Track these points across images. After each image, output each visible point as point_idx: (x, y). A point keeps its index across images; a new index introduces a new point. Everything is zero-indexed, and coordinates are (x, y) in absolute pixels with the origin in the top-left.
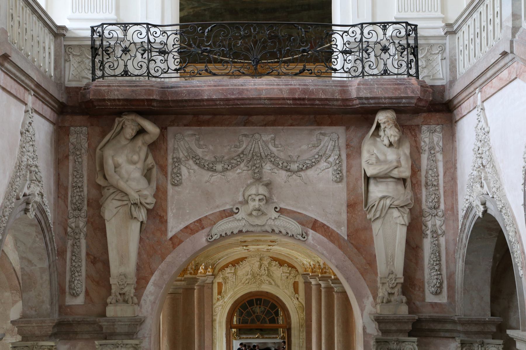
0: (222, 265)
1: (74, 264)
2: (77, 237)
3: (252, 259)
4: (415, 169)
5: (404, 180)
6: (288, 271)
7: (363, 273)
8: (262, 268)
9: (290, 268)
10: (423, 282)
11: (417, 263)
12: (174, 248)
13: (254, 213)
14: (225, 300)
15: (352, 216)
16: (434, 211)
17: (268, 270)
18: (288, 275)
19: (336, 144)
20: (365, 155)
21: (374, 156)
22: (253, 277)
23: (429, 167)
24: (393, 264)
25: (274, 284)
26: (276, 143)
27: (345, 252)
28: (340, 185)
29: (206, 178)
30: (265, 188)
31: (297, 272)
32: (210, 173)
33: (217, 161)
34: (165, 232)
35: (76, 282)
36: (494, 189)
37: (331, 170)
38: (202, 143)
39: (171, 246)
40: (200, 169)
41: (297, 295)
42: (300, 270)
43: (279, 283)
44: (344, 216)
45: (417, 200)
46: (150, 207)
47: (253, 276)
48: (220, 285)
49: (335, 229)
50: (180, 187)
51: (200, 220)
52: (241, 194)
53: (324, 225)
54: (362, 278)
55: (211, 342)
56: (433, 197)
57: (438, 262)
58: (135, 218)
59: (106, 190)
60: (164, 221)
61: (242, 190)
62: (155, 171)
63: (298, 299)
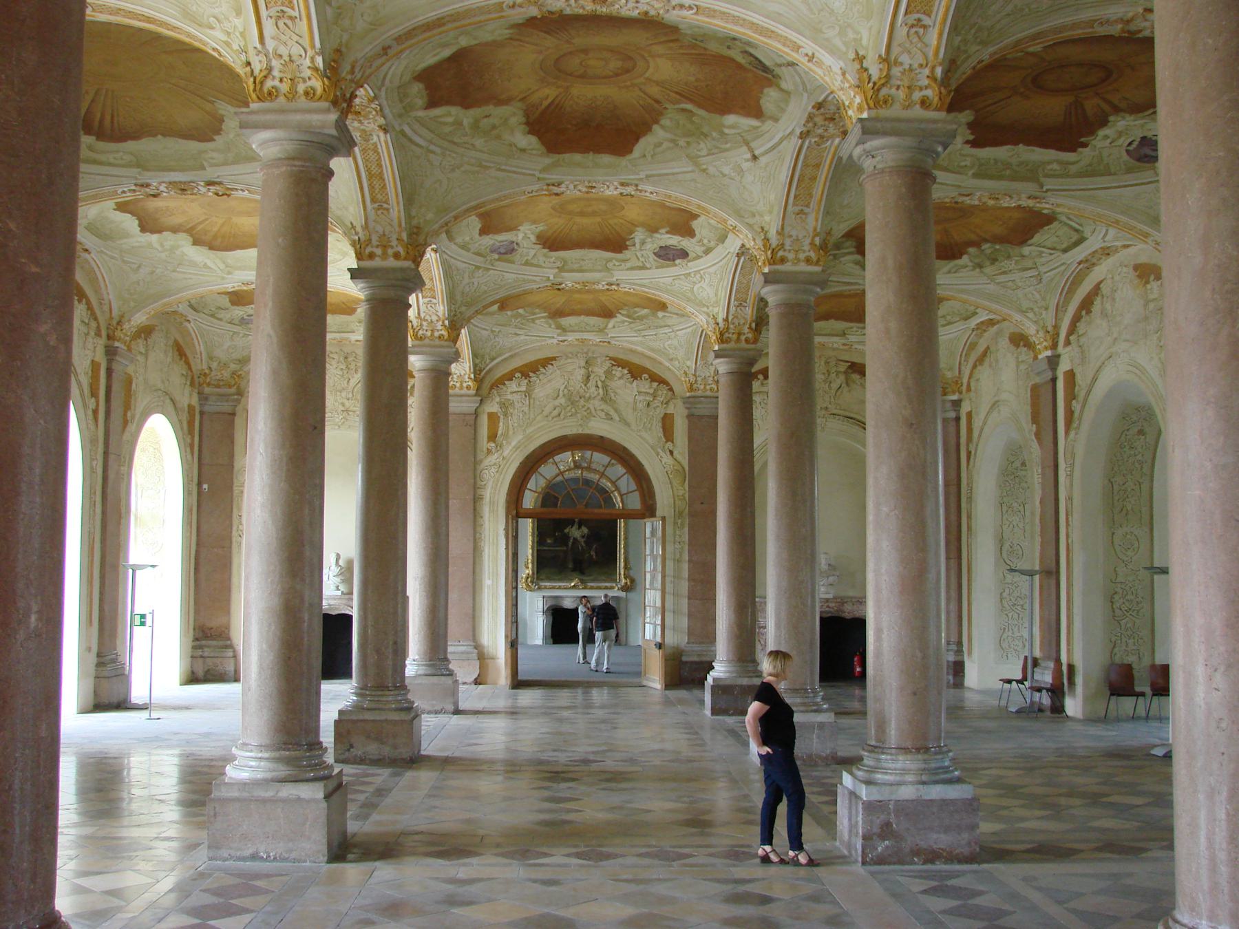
3: (569, 361)
6: (651, 391)
8: (592, 384)
9: (655, 384)
14: (505, 454)
17: (605, 387)
18: (650, 398)
22: (569, 403)
25: (618, 419)
31: (670, 393)
42: (681, 389)
43: (631, 418)
48: (493, 418)
55: (471, 545)
63: (671, 453)
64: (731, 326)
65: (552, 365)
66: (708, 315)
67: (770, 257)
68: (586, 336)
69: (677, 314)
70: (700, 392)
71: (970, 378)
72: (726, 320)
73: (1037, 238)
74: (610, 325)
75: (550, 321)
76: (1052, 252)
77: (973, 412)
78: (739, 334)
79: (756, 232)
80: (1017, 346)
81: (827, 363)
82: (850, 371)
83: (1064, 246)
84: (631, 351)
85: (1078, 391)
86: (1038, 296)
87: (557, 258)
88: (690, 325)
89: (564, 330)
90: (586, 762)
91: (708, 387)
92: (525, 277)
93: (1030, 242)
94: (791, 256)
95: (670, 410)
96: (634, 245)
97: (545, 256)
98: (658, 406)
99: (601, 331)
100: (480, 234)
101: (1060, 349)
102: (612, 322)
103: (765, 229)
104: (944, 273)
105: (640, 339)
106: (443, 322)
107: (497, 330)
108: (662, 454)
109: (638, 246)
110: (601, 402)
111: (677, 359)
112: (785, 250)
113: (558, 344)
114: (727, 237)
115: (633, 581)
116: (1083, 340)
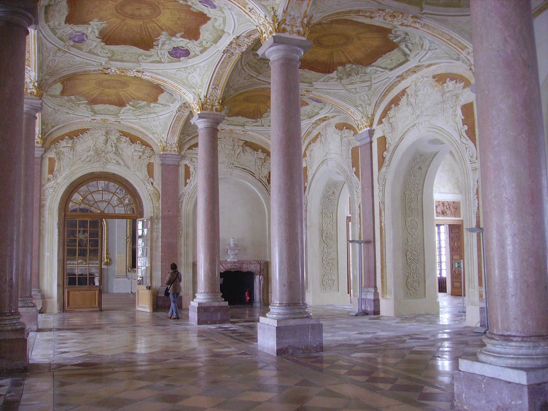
0: (56, 137)
3: (97, 131)
6: (142, 150)
14: (59, 181)
17: (116, 147)
25: (123, 164)
42: (158, 149)
47: (96, 152)
48: (51, 161)
63: (152, 184)
64: (208, 101)
65: (87, 133)
66: (195, 94)
67: (277, 27)
68: (107, 117)
69: (162, 105)
70: (168, 151)
71: (305, 150)
72: (206, 97)
73: (380, 61)
74: (122, 112)
75: (88, 106)
76: (383, 70)
77: (308, 166)
78: (212, 106)
79: (268, 11)
80: (341, 129)
81: (233, 140)
82: (245, 145)
83: (392, 66)
84: (132, 128)
85: (389, 146)
86: (366, 97)
87: (109, 50)
88: (169, 111)
89: (96, 113)
91: (173, 149)
92: (87, 61)
93: (373, 64)
94: (288, 28)
95: (152, 161)
96: (158, 45)
97: (102, 48)
98: (145, 158)
99: (116, 115)
100: (65, 23)
101: (374, 126)
102: (123, 109)
103: (275, 9)
104: (321, 82)
105: (137, 121)
106: (34, 83)
107: (57, 109)
108: (147, 184)
109: (160, 46)
110: (114, 155)
111: (157, 133)
112: (286, 24)
113: (90, 121)
114: (221, 37)
115: (110, 260)
116: (391, 121)
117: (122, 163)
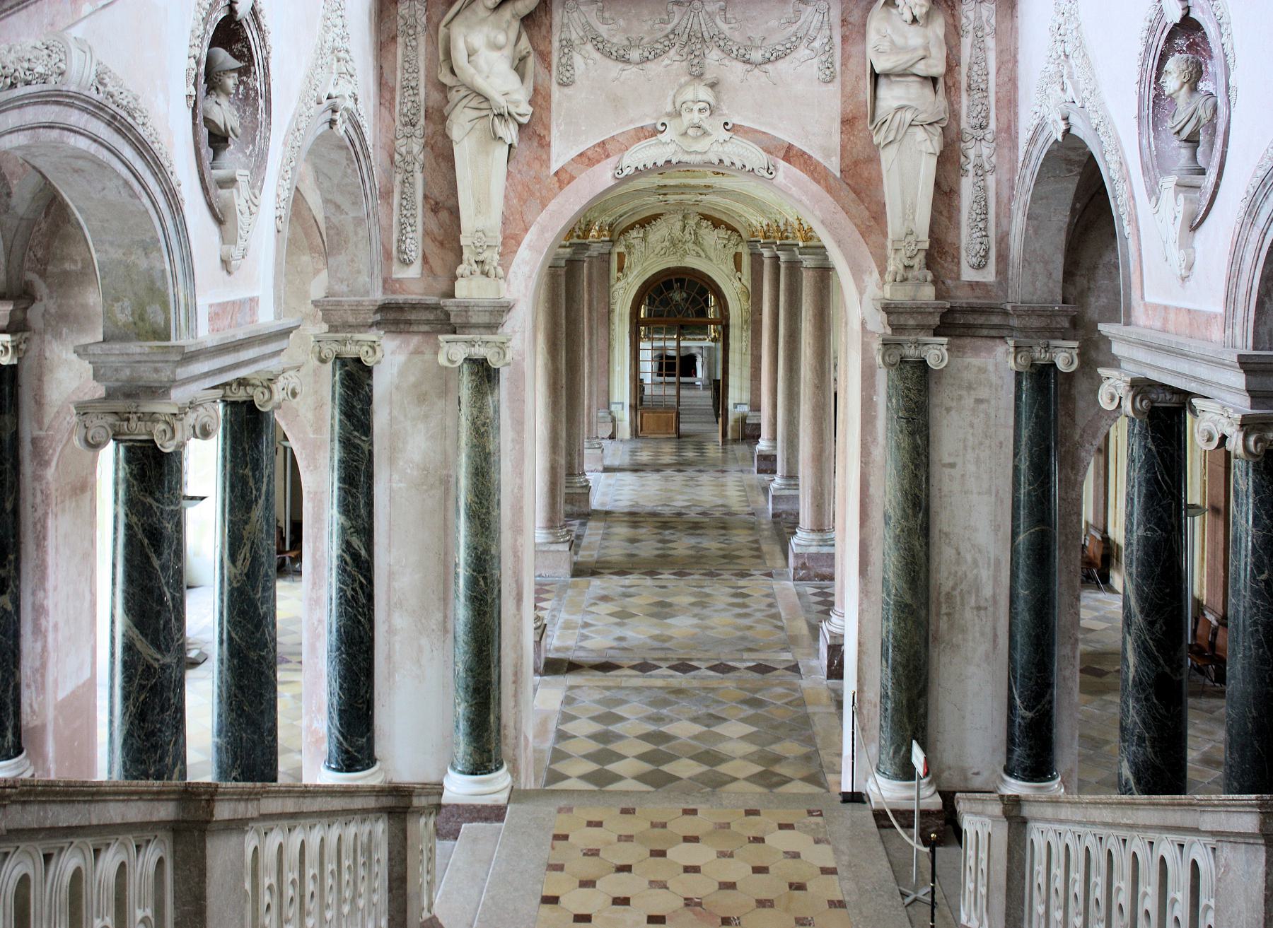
1: (405, 212)
2: (409, 168)
4: (952, 65)
5: (934, 80)
7: (865, 233)
10: (958, 248)
11: (950, 218)
12: (561, 188)
13: (691, 132)
15: (849, 139)
16: (980, 133)
17: (696, 234)
18: (725, 242)
19: (826, 19)
20: (873, 37)
21: (888, 39)
23: (974, 59)
24: (914, 219)
26: (728, 16)
27: (837, 198)
28: (830, 85)
29: (614, 74)
30: (710, 90)
32: (621, 65)
33: (632, 44)
34: (546, 162)
35: (408, 240)
36: (1086, 94)
37: (816, 60)
38: (607, 15)
39: (557, 185)
40: (604, 58)
41: (739, 273)
43: (712, 255)
44: (836, 139)
45: (954, 114)
46: (524, 120)
49: (821, 160)
50: (571, 88)
51: (603, 142)
52: (669, 100)
53: (804, 153)
54: (862, 240)
56: (979, 108)
57: (983, 216)
58: (500, 138)
59: (454, 92)
60: (544, 144)
61: (671, 93)
62: (531, 61)
63: (740, 279)
90: (679, 514)
94: (791, 235)
95: (740, 249)
117: (703, 254)
